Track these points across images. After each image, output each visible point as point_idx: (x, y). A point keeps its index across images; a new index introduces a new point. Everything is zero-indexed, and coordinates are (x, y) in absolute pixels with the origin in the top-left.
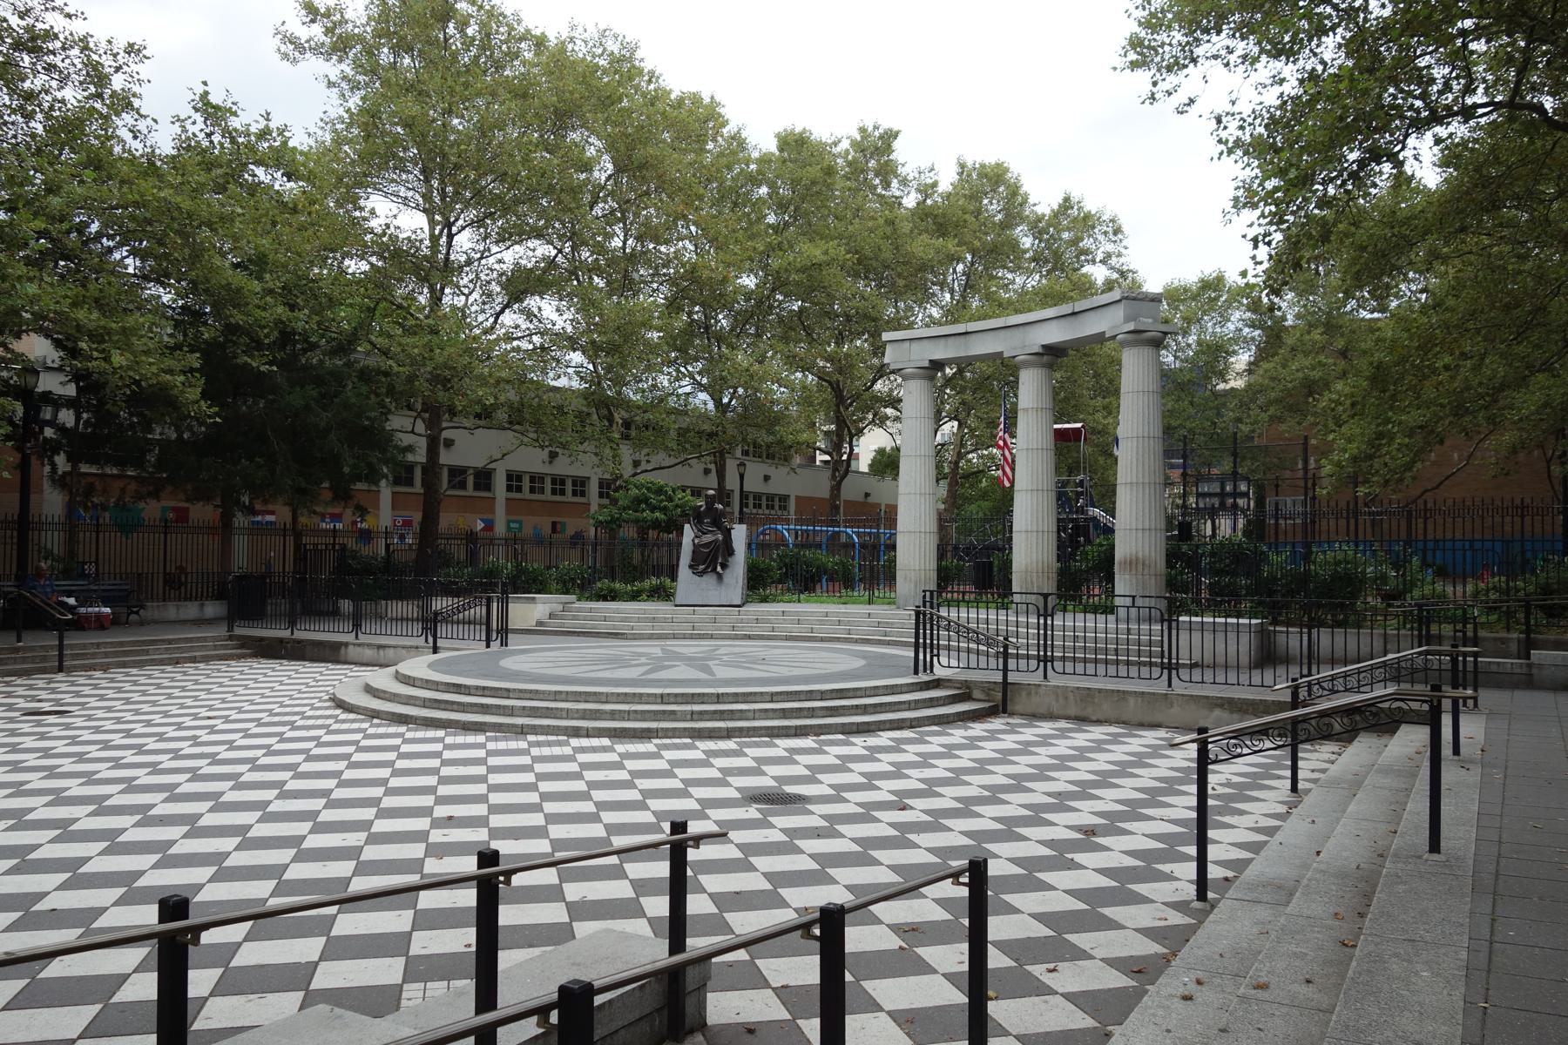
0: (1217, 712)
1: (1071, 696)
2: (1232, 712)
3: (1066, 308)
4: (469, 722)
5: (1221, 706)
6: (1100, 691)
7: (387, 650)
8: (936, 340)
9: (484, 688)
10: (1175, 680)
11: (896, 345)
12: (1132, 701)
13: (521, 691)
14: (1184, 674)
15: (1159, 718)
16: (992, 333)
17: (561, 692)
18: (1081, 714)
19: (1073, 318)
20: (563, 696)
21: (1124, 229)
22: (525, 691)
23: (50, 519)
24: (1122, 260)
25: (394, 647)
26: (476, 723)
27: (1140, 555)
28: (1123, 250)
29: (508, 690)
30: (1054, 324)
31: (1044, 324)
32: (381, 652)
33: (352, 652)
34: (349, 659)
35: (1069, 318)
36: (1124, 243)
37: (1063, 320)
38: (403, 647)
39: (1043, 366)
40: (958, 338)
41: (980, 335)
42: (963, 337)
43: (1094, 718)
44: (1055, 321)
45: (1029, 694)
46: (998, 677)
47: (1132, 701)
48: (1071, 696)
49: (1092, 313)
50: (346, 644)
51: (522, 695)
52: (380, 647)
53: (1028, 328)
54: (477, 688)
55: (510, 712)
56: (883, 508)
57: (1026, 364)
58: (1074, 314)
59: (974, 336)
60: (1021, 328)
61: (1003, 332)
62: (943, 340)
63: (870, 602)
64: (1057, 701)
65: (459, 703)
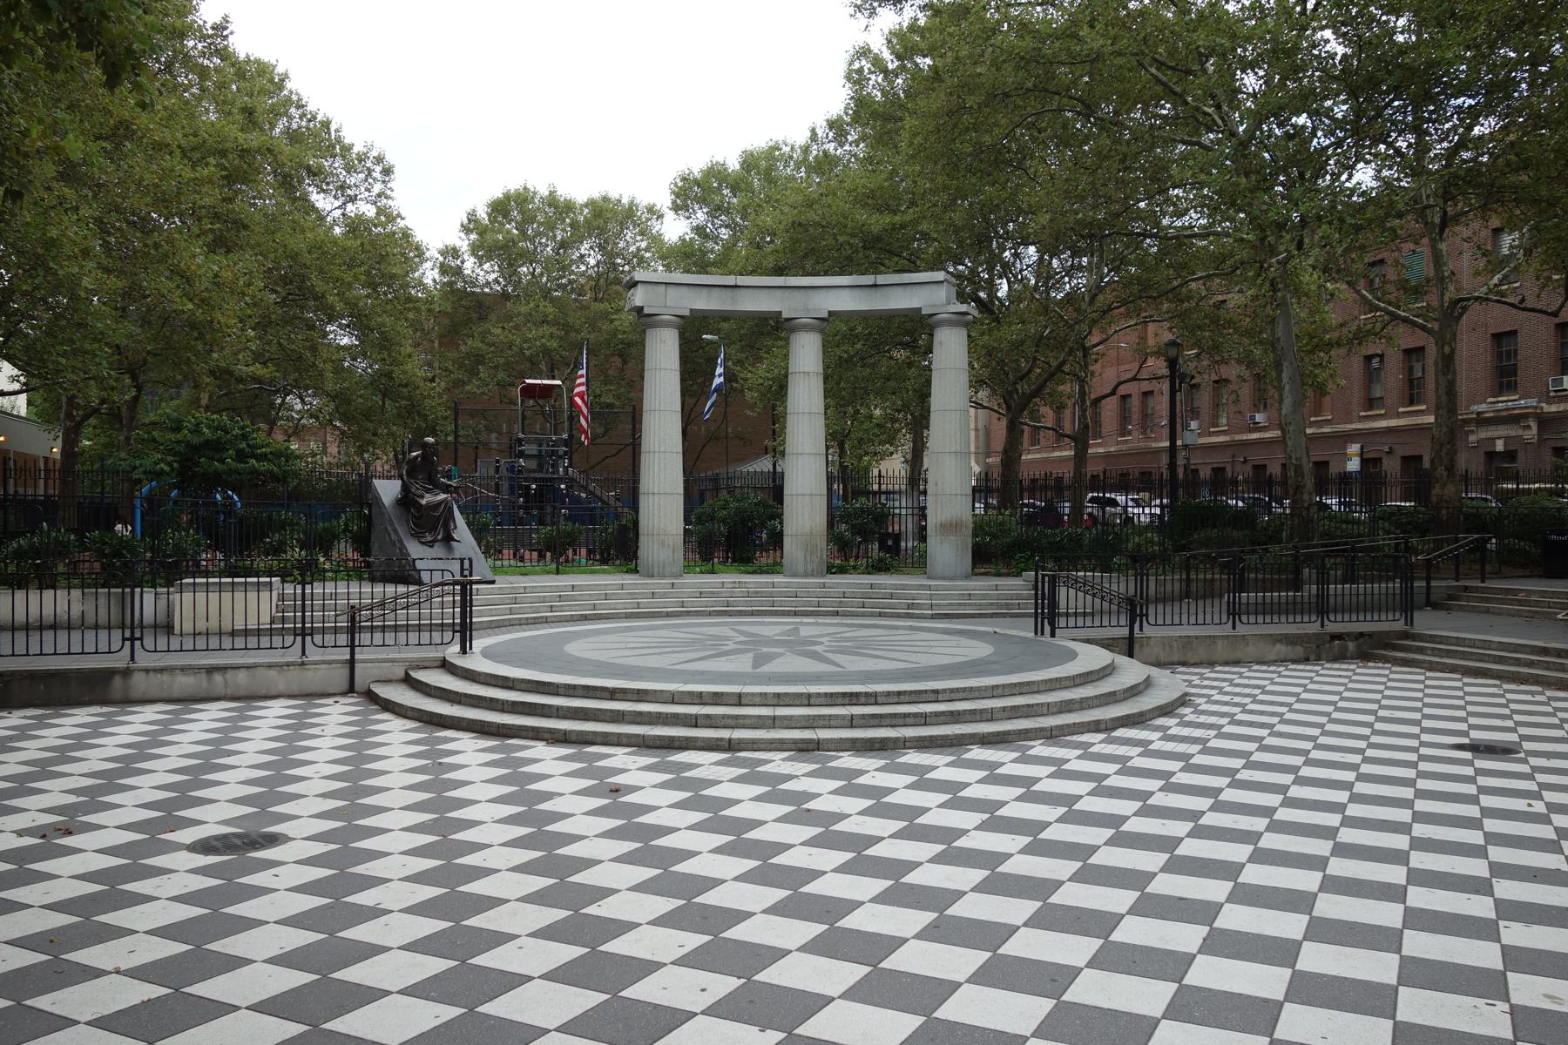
0: (1278, 647)
1: (1175, 644)
2: (1287, 644)
3: (868, 279)
4: (992, 734)
5: (1280, 641)
6: (1197, 637)
7: (230, 674)
8: (698, 289)
9: (899, 693)
10: (138, 651)
11: (649, 287)
12: (1220, 643)
13: (952, 691)
14: (318, 638)
15: (1238, 655)
16: (766, 291)
17: (997, 686)
18: (1182, 659)
19: (873, 289)
20: (1000, 691)
21: (395, 170)
22: (957, 690)
23: (890, 473)
24: (390, 202)
25: (248, 667)
26: (999, 733)
27: (964, 518)
28: (389, 192)
29: (936, 692)
30: (846, 292)
31: (833, 291)
32: (218, 678)
33: (139, 683)
34: (135, 694)
35: (868, 290)
36: (389, 185)
37: (857, 292)
38: (270, 666)
39: (821, 331)
40: (724, 290)
41: (750, 290)
42: (729, 290)
43: (1192, 662)
44: (847, 290)
45: (1142, 646)
46: (1125, 632)
47: (1220, 643)
48: (1175, 644)
49: (899, 290)
50: (126, 673)
51: (953, 696)
52: (211, 670)
53: (811, 292)
54: (888, 694)
55: (989, 716)
56: (12, 456)
57: (806, 328)
58: (875, 286)
59: (743, 290)
60: (802, 291)
61: (778, 293)
62: (705, 291)
63: (558, 572)
64: (1164, 650)
65: (916, 715)
